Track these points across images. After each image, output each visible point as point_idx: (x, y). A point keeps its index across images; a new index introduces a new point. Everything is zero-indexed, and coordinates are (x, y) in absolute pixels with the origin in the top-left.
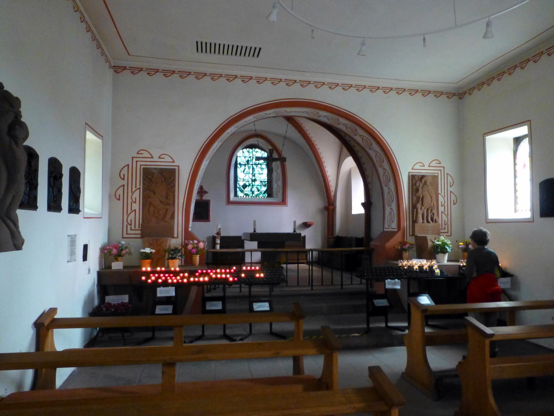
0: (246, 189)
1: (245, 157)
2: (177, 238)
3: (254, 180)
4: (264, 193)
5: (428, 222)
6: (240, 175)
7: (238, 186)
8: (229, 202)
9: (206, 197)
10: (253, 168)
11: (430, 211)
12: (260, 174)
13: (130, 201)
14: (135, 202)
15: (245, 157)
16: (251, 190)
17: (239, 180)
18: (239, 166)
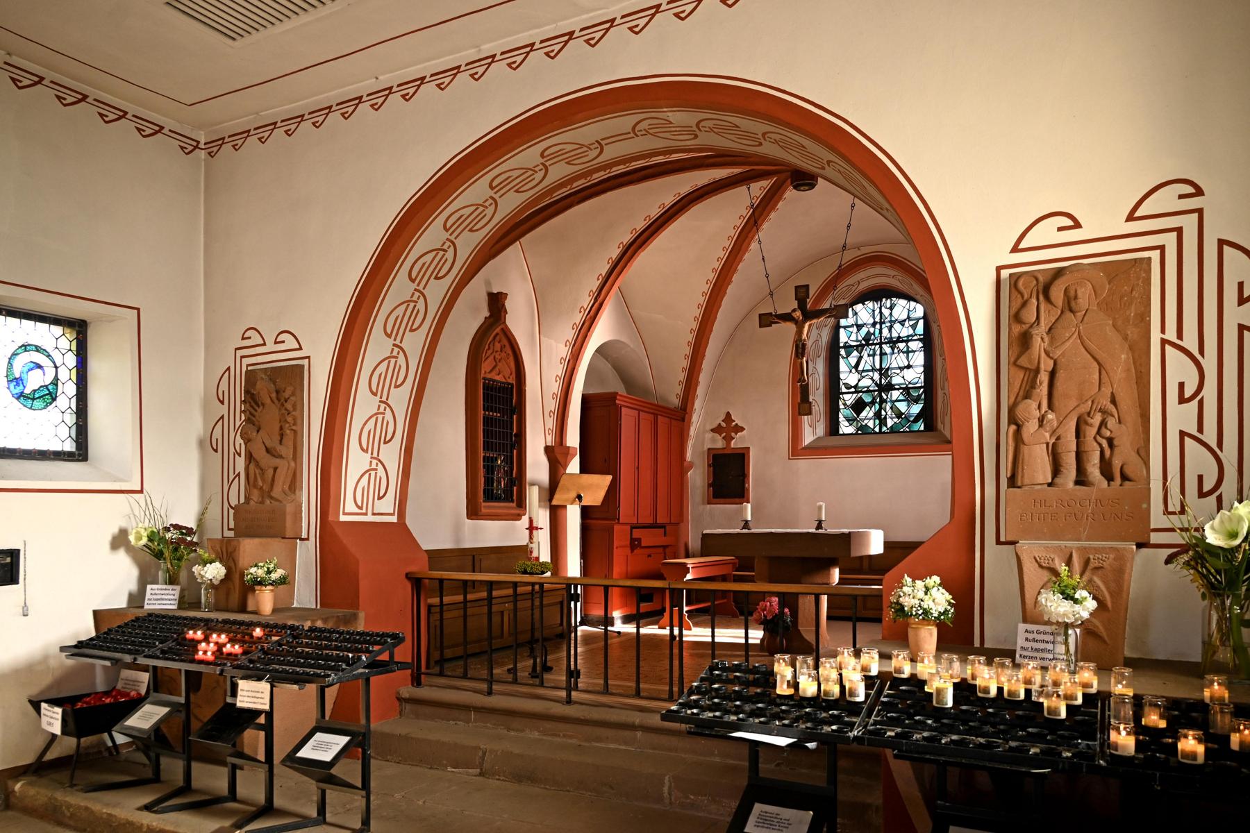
0: (863, 414)
1: (859, 327)
2: (307, 539)
3: (890, 387)
4: (916, 421)
5: (1082, 480)
6: (848, 377)
7: (841, 406)
8: (797, 450)
9: (737, 442)
10: (882, 354)
11: (1091, 432)
12: (902, 369)
13: (232, 450)
14: (239, 455)
16: (877, 415)
17: (844, 390)
18: (842, 352)
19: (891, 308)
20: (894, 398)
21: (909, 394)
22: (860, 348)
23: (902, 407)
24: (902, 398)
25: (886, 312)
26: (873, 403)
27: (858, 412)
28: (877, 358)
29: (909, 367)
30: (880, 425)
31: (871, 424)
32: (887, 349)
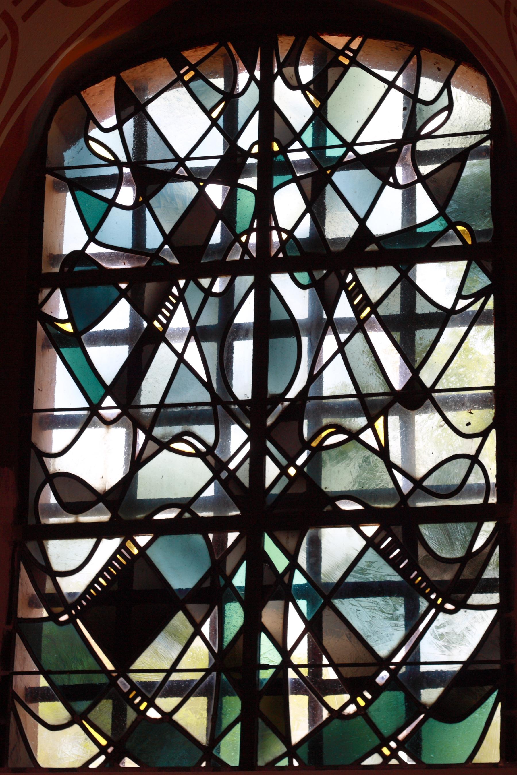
0: (155, 658)
3: (310, 508)
12: (372, 406)
15: (149, 180)
16: (234, 665)
19: (320, 91)
20: (332, 568)
21: (411, 542)
22: (148, 280)
23: (379, 625)
24: (381, 571)
25: (294, 106)
26: (211, 593)
27: (126, 648)
28: (243, 351)
29: (415, 397)
30: (248, 721)
31: (193, 716)
32: (296, 298)
